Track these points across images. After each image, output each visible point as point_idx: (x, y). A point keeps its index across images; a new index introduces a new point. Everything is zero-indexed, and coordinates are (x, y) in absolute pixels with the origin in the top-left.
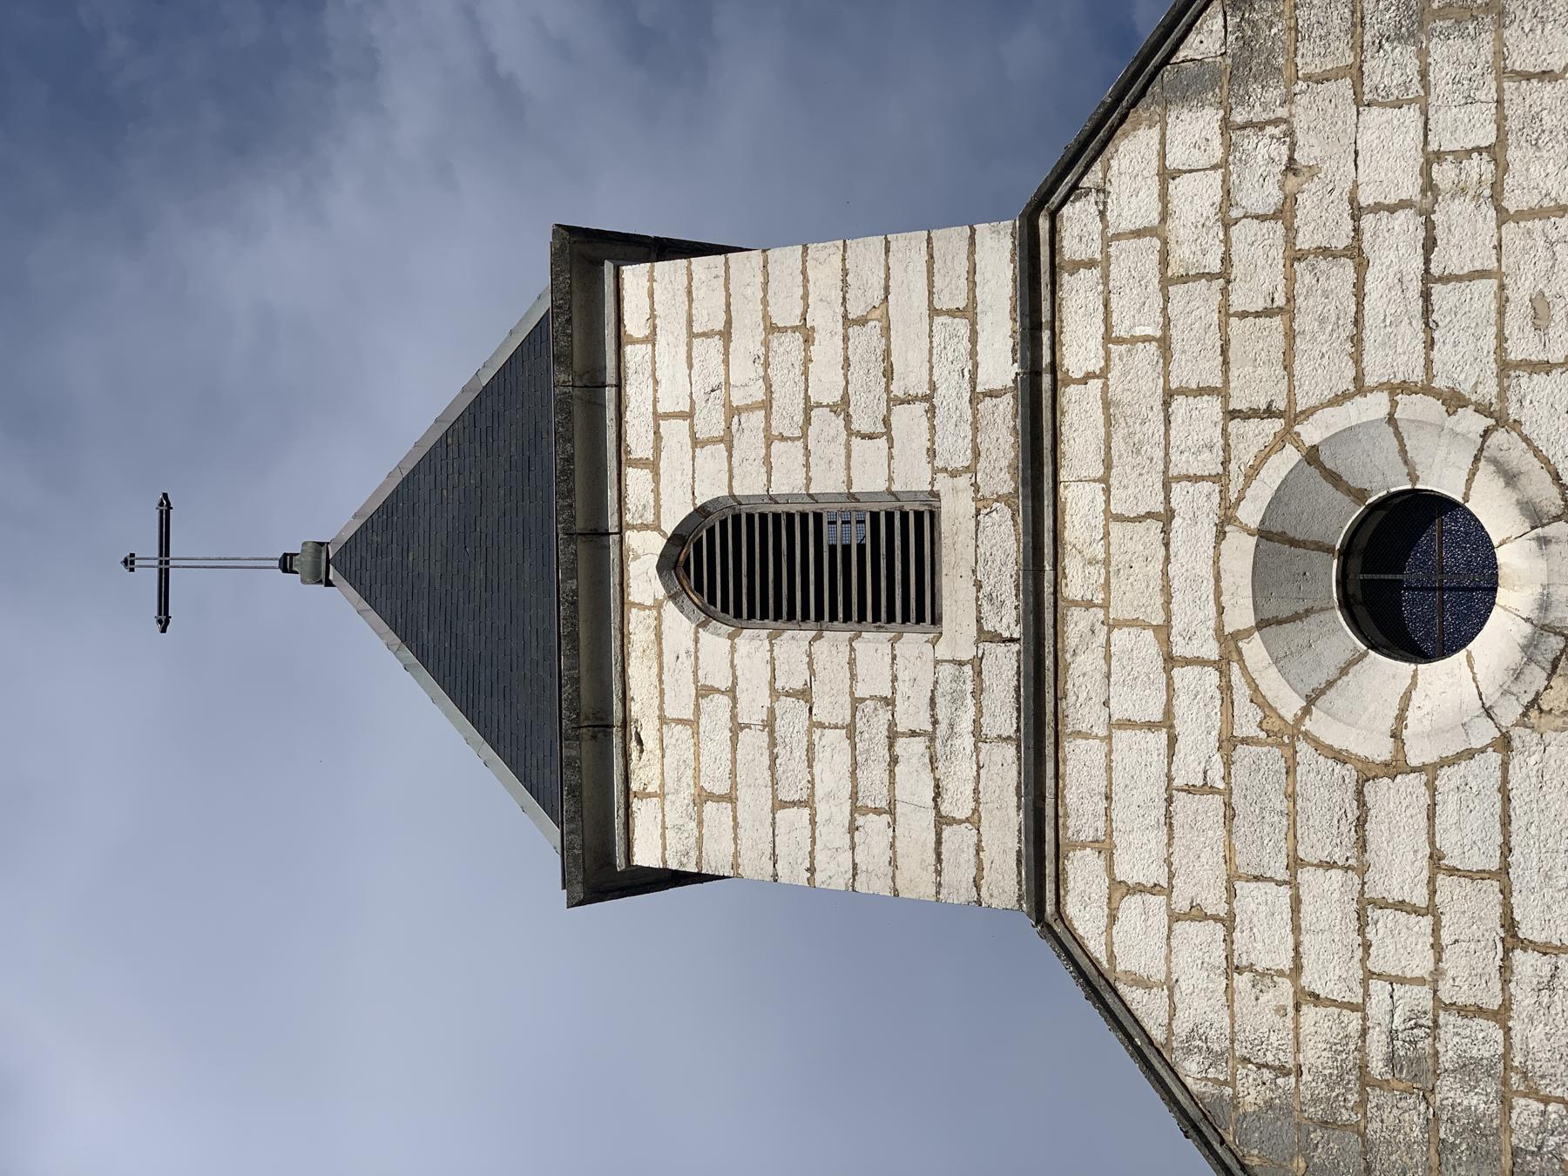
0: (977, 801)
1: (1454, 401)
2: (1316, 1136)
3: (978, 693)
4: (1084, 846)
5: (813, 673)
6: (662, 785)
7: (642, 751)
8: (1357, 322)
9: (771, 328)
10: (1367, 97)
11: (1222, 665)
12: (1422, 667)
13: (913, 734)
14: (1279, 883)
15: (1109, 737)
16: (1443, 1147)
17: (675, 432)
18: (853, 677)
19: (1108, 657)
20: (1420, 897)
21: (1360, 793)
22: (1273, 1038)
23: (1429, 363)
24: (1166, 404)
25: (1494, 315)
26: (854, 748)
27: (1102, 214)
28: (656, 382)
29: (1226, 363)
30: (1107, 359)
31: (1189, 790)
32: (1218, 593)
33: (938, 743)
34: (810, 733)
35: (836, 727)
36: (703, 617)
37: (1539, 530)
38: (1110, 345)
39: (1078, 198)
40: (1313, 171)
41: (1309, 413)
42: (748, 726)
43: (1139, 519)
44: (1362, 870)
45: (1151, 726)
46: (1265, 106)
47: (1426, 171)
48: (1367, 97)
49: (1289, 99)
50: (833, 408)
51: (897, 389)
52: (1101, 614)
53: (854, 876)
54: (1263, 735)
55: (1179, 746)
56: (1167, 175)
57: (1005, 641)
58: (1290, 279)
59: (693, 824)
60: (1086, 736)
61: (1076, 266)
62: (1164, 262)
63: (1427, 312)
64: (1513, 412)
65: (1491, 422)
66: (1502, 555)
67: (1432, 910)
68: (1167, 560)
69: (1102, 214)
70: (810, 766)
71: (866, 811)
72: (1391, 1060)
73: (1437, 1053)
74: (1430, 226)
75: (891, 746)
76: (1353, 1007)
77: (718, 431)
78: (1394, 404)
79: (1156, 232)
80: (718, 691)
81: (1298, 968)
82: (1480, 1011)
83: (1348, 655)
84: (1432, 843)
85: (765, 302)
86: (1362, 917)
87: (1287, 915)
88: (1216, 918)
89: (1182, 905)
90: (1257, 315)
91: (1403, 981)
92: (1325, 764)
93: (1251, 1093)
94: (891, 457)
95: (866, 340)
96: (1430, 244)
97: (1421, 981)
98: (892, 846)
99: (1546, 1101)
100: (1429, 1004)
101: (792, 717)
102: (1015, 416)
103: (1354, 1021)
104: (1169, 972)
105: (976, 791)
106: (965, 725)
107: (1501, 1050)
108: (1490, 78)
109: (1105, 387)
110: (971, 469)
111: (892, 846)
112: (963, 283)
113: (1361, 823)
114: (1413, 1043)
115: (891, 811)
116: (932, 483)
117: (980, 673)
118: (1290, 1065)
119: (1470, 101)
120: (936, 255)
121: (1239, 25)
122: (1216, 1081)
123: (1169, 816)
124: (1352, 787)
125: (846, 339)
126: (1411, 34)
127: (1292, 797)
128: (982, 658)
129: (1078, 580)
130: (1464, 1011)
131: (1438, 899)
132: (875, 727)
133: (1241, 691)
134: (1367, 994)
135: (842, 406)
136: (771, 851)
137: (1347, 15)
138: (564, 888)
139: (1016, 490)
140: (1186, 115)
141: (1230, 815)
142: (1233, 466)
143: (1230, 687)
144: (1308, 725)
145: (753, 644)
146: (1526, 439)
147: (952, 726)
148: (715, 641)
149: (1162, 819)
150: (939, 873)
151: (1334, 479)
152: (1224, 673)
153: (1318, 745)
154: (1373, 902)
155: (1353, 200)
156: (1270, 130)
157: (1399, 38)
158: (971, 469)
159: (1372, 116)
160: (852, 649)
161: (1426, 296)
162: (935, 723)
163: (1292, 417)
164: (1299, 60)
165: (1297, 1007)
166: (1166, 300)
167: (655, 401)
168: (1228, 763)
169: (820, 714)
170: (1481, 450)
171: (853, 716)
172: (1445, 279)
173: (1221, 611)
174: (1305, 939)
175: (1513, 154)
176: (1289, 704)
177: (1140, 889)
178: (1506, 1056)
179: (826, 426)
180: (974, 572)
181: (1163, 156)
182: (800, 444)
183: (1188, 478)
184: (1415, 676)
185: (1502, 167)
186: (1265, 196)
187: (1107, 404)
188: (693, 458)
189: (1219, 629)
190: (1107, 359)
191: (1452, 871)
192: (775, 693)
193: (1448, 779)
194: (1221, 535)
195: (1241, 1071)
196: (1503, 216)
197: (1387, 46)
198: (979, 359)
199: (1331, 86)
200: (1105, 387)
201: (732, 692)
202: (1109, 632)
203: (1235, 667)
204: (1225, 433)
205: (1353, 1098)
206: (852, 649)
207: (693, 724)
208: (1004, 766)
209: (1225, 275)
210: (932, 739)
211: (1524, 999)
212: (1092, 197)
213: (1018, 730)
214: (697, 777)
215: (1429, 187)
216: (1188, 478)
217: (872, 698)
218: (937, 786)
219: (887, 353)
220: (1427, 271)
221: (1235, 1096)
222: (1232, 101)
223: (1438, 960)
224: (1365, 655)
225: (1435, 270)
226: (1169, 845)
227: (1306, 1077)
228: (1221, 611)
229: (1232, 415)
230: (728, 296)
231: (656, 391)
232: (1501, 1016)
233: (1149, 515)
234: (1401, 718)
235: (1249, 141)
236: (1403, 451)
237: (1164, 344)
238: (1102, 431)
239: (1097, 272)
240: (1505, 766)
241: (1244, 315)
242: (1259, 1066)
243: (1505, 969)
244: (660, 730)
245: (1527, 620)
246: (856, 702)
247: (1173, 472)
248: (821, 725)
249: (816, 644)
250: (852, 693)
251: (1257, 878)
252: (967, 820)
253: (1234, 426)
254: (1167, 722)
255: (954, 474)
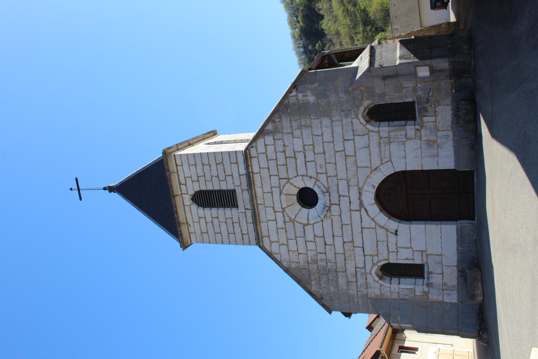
0: (248, 231)
1: (311, 177)
2: (303, 270)
3: (246, 217)
4: (265, 237)
5: (218, 215)
6: (195, 231)
7: (190, 227)
8: (296, 167)
9: (203, 164)
10: (294, 137)
11: (283, 212)
12: (310, 210)
13: (236, 223)
14: (294, 240)
15: (267, 222)
16: (319, 270)
17: (189, 180)
18: (225, 215)
19: (266, 211)
20: (313, 240)
21: (304, 228)
22: (295, 259)
23: (307, 173)
24: (270, 177)
25: (315, 167)
26: (227, 225)
27: (257, 150)
28: (184, 172)
29: (278, 172)
30: (260, 170)
31: (280, 228)
32: (281, 203)
33: (241, 224)
34: (219, 223)
35: (223, 222)
36: (197, 206)
37: (324, 194)
38: (260, 169)
39: (252, 148)
40: (287, 146)
41: (291, 178)
42: (208, 222)
43: (268, 193)
44: (305, 237)
45: (273, 220)
46: (279, 137)
47: (304, 147)
48: (294, 137)
49: (283, 136)
50: (216, 176)
51: (227, 174)
52: (264, 206)
53: (230, 242)
54: (290, 221)
55: (278, 223)
56: (266, 145)
57: (249, 209)
58: (286, 161)
59: (201, 237)
60: (264, 222)
61: (254, 157)
62: (267, 157)
63: (306, 166)
64: (319, 179)
65: (316, 180)
66: (318, 195)
67: (315, 241)
68: (273, 198)
69: (257, 150)
70: (220, 227)
71: (230, 233)
72: (312, 260)
73: (317, 259)
74: (305, 154)
75: (233, 224)
76: (306, 254)
77: (196, 180)
78: (303, 178)
79: (265, 153)
80: (202, 218)
81: (298, 250)
82: (322, 253)
83: (299, 209)
84: (314, 233)
85: (202, 161)
86: (306, 243)
87: (296, 243)
88: (286, 245)
89: (281, 243)
90: (282, 165)
91: (312, 250)
92: (299, 224)
93: (293, 265)
94: (227, 184)
95: (220, 167)
96: (305, 157)
97: (314, 250)
98: (235, 238)
99: (332, 263)
100: (316, 253)
101: (216, 221)
102: (247, 178)
103: (306, 256)
104: (280, 252)
105: (247, 230)
106: (245, 221)
107: (325, 257)
108: (311, 135)
109: (260, 175)
110: (240, 185)
111: (235, 238)
112: (235, 159)
113: (304, 231)
114: (314, 258)
115: (234, 233)
116: (234, 188)
117: (246, 214)
118: (298, 262)
119: (309, 138)
120: (230, 154)
121: (274, 125)
122: (288, 265)
123: (277, 232)
124: (303, 227)
125: (217, 166)
126: (299, 129)
127: (294, 228)
128: (246, 212)
129: (260, 201)
130: (320, 253)
131: (316, 240)
132: (230, 222)
133: (286, 216)
134: (307, 252)
135: (218, 176)
136: (215, 240)
137: (290, 125)
138: (181, 247)
139: (248, 188)
140: (267, 137)
141: (286, 231)
142: (281, 186)
143: (284, 215)
144: (296, 219)
145: (207, 210)
146: (321, 182)
147: (242, 221)
148: (201, 210)
149: (277, 233)
150: (243, 241)
151: (295, 186)
152: (283, 213)
153: (297, 222)
154: (307, 241)
155: (294, 150)
156: (280, 140)
157: (298, 129)
158: (240, 185)
159: (295, 139)
160: (224, 211)
161: (305, 164)
162: (240, 221)
163: (289, 179)
164: (284, 131)
165: (298, 255)
166: (268, 163)
167: (184, 175)
168: (285, 225)
169: (220, 220)
170: (315, 183)
171: (226, 220)
172: (308, 162)
173: (282, 205)
174: (298, 246)
175: (315, 146)
176: (293, 217)
177: (274, 242)
178: (326, 258)
179: (215, 180)
180: (243, 200)
181: (265, 143)
182: (211, 182)
183: (275, 187)
184: (309, 211)
185: (314, 147)
186: (282, 149)
187: (261, 177)
188: (193, 184)
189: (282, 207)
190: (260, 170)
191: (317, 237)
192: (212, 218)
193: (315, 225)
194: (280, 195)
195: (291, 263)
196: (315, 154)
197: (296, 130)
198: (240, 170)
199: (289, 134)
200: (260, 175)
201: (205, 218)
202: (265, 208)
203: (285, 212)
204: (279, 181)
205: (307, 265)
206: (224, 211)
207: (199, 222)
208: (251, 227)
209: (276, 159)
210: (239, 223)
211: (328, 251)
212: (255, 147)
213: (253, 222)
214: (201, 230)
215: (304, 149)
216: (275, 187)
217: (229, 218)
218: (241, 230)
219: (224, 169)
220: (305, 160)
221: (291, 267)
222: (274, 136)
223: (316, 247)
224: (301, 209)
225: (306, 160)
226: (278, 236)
227: (300, 263)
228: (282, 205)
229: (280, 179)
230: (195, 159)
231: (184, 174)
232: (325, 253)
233: (269, 192)
234: (308, 217)
235: (277, 141)
236: (304, 183)
237: (269, 169)
238: (261, 181)
239: (257, 158)
240: (322, 224)
241: (280, 165)
242: (294, 262)
243: (325, 248)
244: (193, 223)
245: (323, 205)
246: (226, 219)
247: (272, 186)
248: (221, 222)
249: (218, 211)
250: (225, 217)
251: (291, 239)
252: (247, 234)
253: (280, 180)
254: (276, 220)
255: (238, 186)
